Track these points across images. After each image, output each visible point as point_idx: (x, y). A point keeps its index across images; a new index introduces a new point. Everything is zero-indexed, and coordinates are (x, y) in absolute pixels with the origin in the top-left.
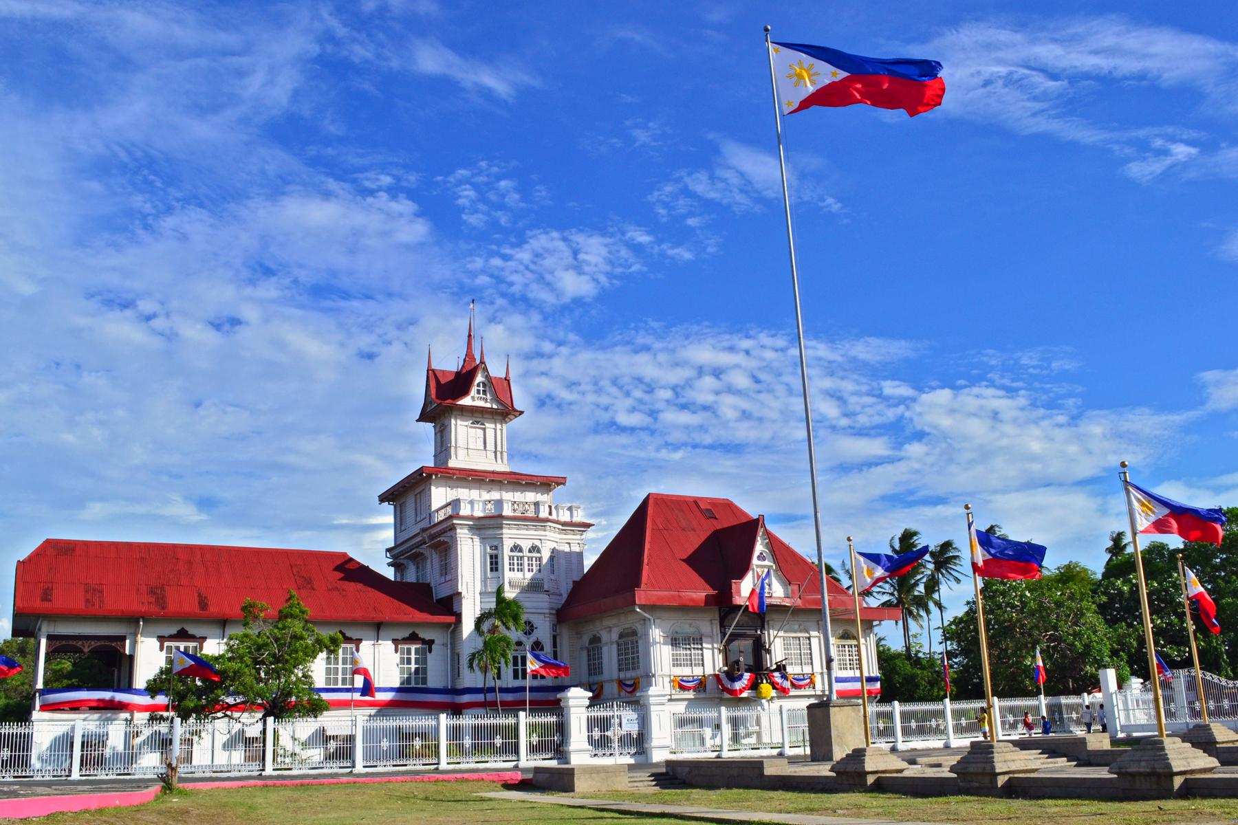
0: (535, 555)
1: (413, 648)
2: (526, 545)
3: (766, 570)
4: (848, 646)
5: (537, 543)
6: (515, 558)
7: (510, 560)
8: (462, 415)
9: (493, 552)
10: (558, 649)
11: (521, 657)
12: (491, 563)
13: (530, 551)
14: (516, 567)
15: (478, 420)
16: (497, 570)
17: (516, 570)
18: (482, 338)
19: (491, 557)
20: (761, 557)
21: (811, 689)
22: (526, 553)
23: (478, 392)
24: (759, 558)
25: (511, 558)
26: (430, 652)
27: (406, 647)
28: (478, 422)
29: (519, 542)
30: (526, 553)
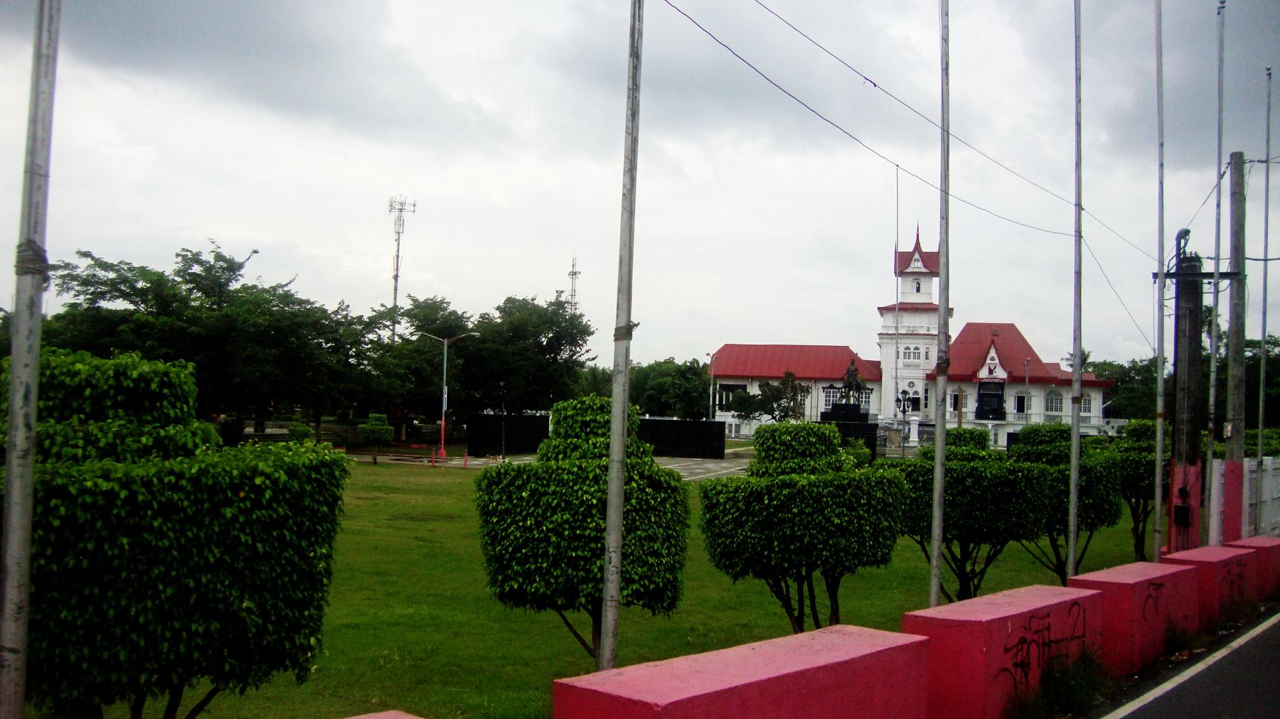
2: (912, 347)
22: (912, 350)
30: (912, 350)
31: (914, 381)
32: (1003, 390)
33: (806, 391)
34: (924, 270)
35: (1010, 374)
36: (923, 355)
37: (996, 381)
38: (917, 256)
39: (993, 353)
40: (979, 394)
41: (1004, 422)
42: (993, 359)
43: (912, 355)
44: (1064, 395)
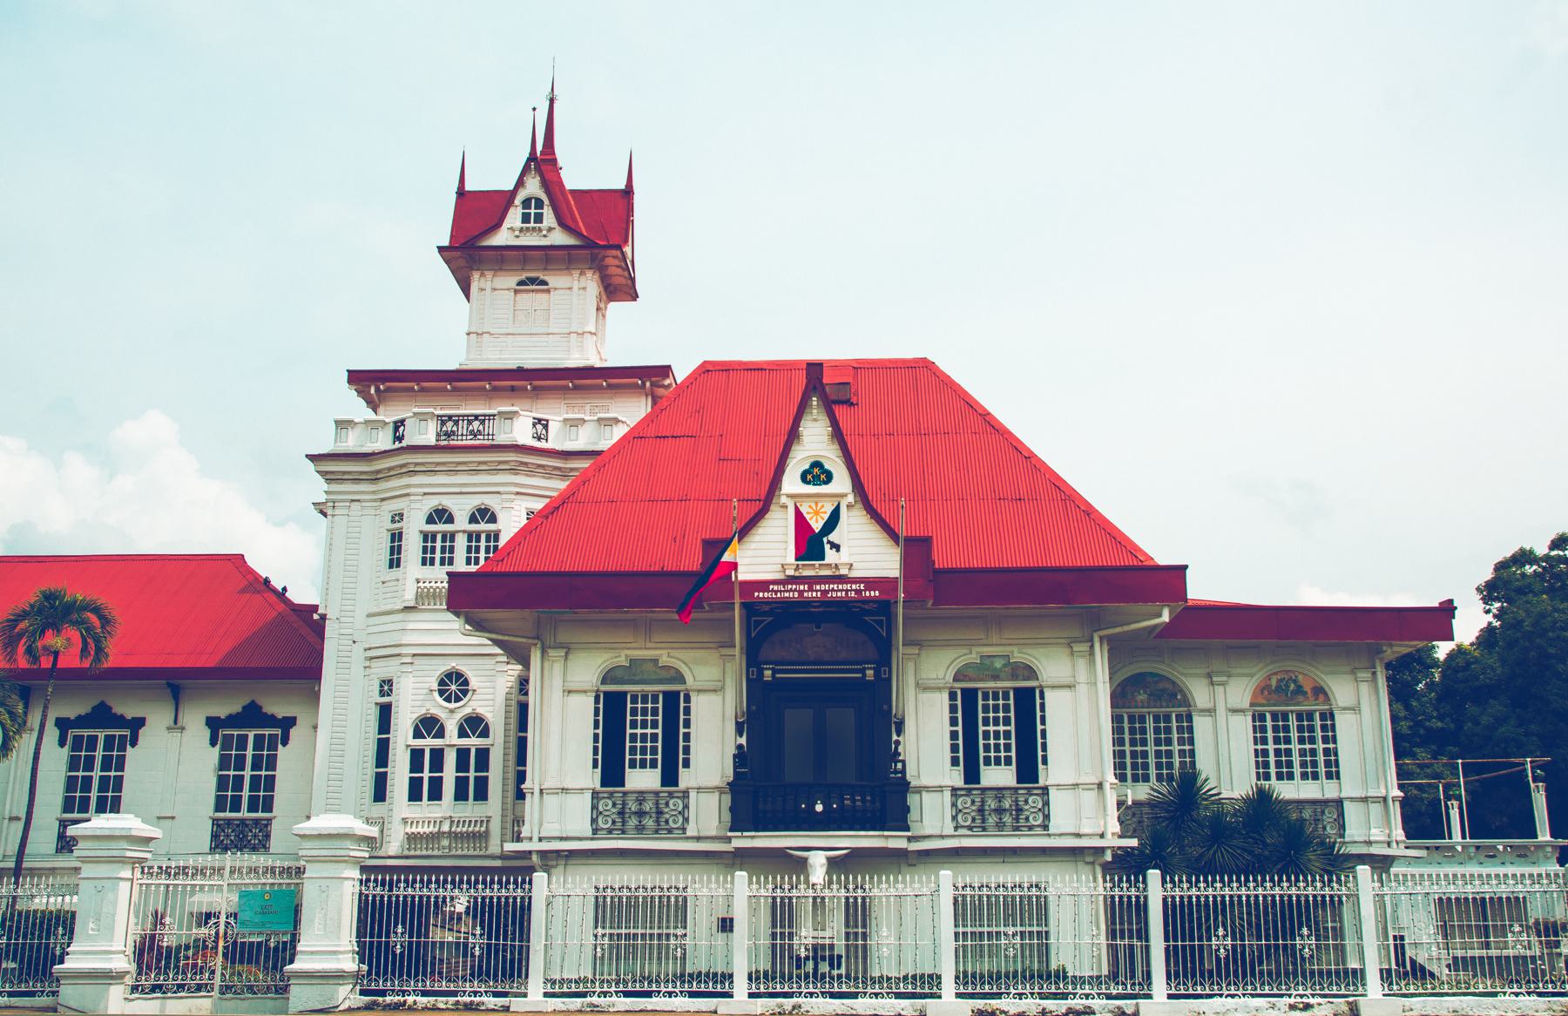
0: (483, 526)
2: (461, 509)
3: (828, 508)
4: (1300, 717)
5: (490, 501)
6: (439, 537)
7: (425, 540)
8: (501, 269)
9: (397, 525)
11: (433, 751)
12: (392, 548)
13: (473, 519)
14: (438, 555)
16: (398, 566)
17: (437, 561)
18: (534, 109)
19: (393, 541)
20: (817, 474)
21: (1039, 831)
22: (461, 523)
23: (526, 219)
24: (805, 478)
25: (428, 537)
26: (285, 742)
28: (533, 281)
29: (448, 502)
30: (461, 523)
31: (463, 666)
32: (884, 659)
34: (559, 238)
35: (915, 549)
37: (838, 592)
39: (815, 440)
41: (895, 841)
43: (461, 543)
44: (1200, 693)
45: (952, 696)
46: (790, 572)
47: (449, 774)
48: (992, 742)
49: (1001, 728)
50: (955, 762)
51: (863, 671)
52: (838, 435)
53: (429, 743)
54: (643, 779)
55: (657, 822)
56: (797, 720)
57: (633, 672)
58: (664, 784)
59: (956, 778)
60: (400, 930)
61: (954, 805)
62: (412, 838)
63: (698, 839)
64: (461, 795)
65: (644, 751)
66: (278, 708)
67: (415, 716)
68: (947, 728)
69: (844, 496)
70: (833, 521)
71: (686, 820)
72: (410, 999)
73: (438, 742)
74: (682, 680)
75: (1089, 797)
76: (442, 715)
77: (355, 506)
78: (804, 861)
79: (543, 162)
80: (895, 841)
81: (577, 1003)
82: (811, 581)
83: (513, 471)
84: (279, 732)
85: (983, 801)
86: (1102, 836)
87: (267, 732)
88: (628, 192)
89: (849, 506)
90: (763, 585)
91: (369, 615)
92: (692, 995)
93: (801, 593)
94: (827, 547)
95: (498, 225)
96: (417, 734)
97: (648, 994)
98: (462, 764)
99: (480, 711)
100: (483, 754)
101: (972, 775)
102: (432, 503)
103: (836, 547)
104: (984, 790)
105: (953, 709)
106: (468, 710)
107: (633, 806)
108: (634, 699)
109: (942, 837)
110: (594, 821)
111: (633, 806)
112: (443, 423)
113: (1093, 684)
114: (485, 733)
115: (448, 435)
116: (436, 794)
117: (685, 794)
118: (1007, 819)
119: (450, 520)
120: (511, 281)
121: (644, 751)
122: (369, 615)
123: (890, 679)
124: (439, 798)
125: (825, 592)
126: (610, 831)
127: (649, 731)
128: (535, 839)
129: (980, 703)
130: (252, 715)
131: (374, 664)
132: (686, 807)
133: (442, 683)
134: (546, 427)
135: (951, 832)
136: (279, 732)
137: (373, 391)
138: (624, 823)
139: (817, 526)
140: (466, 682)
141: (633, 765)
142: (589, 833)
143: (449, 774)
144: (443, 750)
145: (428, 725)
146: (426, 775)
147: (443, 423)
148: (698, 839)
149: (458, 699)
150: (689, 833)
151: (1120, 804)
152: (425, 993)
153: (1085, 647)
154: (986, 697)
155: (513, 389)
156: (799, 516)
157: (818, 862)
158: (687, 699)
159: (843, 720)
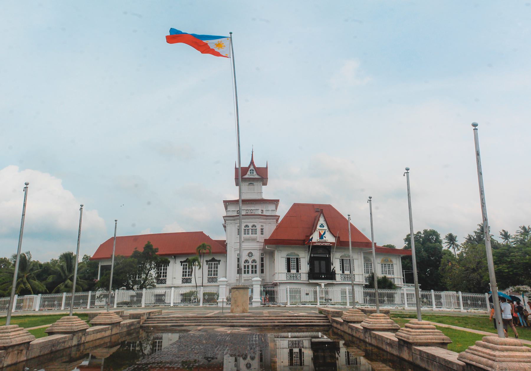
0: (254, 228)
1: (213, 263)
2: (250, 225)
3: (324, 231)
5: (255, 224)
10: (264, 262)
11: (247, 266)
13: (252, 227)
14: (246, 233)
15: (251, 183)
17: (246, 234)
22: (250, 227)
23: (251, 173)
24: (320, 226)
26: (219, 264)
27: (210, 263)
28: (251, 184)
30: (250, 227)
31: (252, 251)
32: (330, 254)
33: (167, 263)
34: (257, 177)
35: (338, 239)
36: (259, 231)
37: (326, 244)
38: (252, 168)
39: (322, 221)
40: (310, 257)
41: (334, 282)
42: (322, 226)
43: (250, 231)
45: (340, 260)
46: (319, 241)
47: (250, 269)
48: (346, 267)
49: (347, 265)
50: (341, 270)
51: (327, 255)
52: (325, 220)
53: (246, 264)
54: (293, 271)
55: (296, 278)
56: (316, 263)
57: (291, 254)
58: (297, 272)
59: (341, 272)
60: (268, 295)
61: (341, 276)
62: (245, 280)
63: (303, 281)
64: (252, 273)
65: (293, 267)
66: (217, 258)
67: (244, 260)
68: (339, 265)
69: (326, 229)
70: (325, 232)
71: (301, 278)
72: (270, 305)
73: (248, 264)
74: (299, 256)
75: (361, 276)
76: (249, 259)
77: (231, 225)
78: (321, 285)
79: (252, 163)
80: (334, 282)
81: (295, 306)
82: (322, 242)
83: (258, 219)
84: (218, 262)
85: (345, 276)
86: (363, 282)
87: (216, 262)
88: (267, 168)
89: (327, 231)
90: (315, 243)
91: (235, 243)
92: (312, 304)
93: (321, 244)
94: (324, 237)
95: (246, 174)
96: (245, 263)
97: (305, 304)
98: (252, 268)
99: (255, 259)
100: (256, 266)
101: (343, 272)
102: (245, 224)
103: (325, 237)
104: (345, 274)
105: (340, 262)
106: (253, 259)
107: (292, 276)
108: (292, 259)
109: (339, 281)
110: (287, 278)
111: (292, 276)
112: (246, 211)
113: (362, 259)
114: (256, 262)
115: (247, 213)
116: (248, 273)
117: (300, 274)
118: (349, 279)
119: (248, 227)
120: (247, 184)
121: (293, 267)
122: (235, 243)
123: (330, 257)
124: (249, 273)
125: (324, 244)
126: (289, 279)
127: (294, 264)
128: (278, 280)
129: (344, 261)
130: (213, 260)
131: (236, 251)
132: (301, 276)
133: (248, 254)
134: (263, 211)
135: (340, 280)
136: (218, 262)
137: (227, 204)
138: (291, 278)
139: (322, 234)
140: (252, 254)
141: (292, 269)
142: (286, 280)
143: (250, 269)
144: (249, 265)
145: (246, 261)
146: (246, 269)
147: (246, 211)
148: (303, 281)
149: (251, 257)
150: (301, 280)
151: (365, 277)
152: (272, 304)
153: (360, 253)
154: (345, 260)
155: (251, 203)
156: (319, 232)
157: (323, 285)
158: (300, 259)
159: (323, 263)
